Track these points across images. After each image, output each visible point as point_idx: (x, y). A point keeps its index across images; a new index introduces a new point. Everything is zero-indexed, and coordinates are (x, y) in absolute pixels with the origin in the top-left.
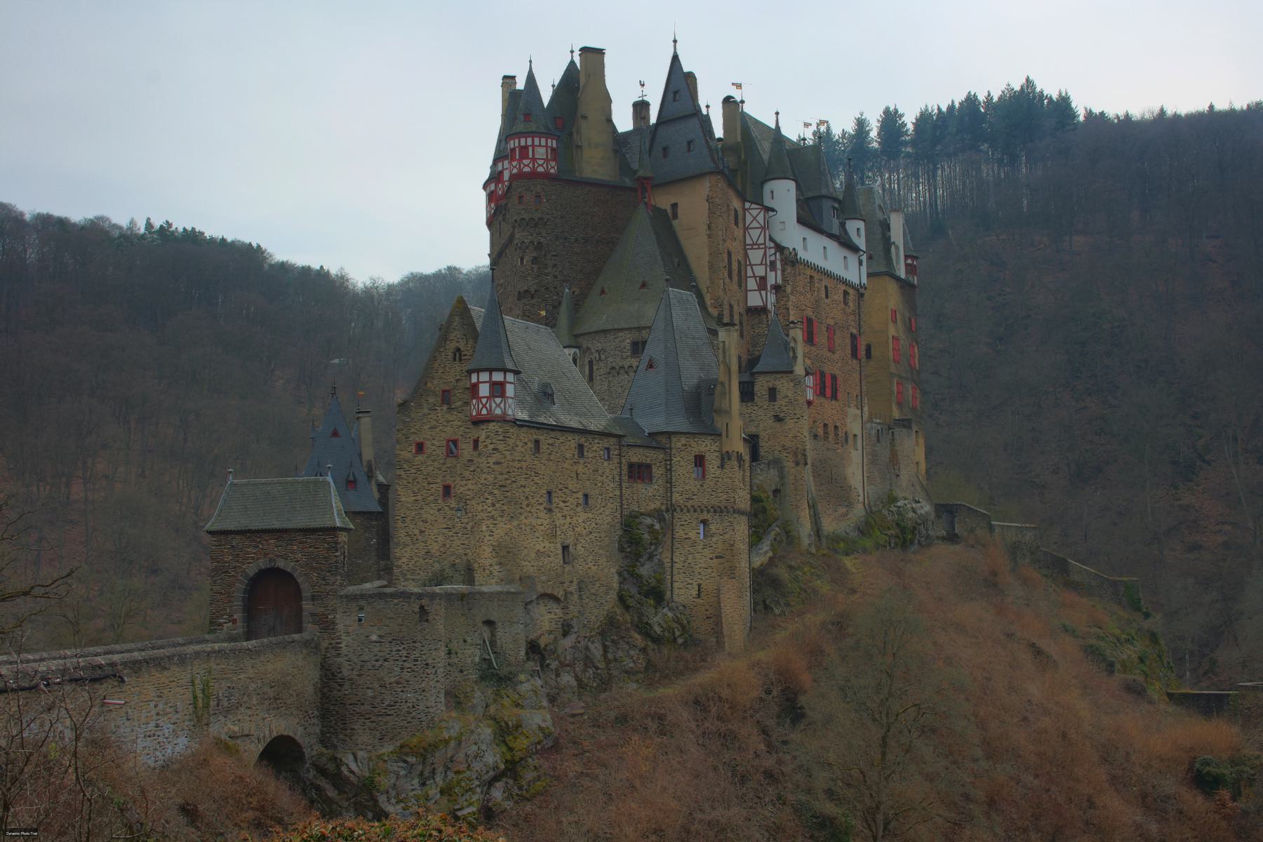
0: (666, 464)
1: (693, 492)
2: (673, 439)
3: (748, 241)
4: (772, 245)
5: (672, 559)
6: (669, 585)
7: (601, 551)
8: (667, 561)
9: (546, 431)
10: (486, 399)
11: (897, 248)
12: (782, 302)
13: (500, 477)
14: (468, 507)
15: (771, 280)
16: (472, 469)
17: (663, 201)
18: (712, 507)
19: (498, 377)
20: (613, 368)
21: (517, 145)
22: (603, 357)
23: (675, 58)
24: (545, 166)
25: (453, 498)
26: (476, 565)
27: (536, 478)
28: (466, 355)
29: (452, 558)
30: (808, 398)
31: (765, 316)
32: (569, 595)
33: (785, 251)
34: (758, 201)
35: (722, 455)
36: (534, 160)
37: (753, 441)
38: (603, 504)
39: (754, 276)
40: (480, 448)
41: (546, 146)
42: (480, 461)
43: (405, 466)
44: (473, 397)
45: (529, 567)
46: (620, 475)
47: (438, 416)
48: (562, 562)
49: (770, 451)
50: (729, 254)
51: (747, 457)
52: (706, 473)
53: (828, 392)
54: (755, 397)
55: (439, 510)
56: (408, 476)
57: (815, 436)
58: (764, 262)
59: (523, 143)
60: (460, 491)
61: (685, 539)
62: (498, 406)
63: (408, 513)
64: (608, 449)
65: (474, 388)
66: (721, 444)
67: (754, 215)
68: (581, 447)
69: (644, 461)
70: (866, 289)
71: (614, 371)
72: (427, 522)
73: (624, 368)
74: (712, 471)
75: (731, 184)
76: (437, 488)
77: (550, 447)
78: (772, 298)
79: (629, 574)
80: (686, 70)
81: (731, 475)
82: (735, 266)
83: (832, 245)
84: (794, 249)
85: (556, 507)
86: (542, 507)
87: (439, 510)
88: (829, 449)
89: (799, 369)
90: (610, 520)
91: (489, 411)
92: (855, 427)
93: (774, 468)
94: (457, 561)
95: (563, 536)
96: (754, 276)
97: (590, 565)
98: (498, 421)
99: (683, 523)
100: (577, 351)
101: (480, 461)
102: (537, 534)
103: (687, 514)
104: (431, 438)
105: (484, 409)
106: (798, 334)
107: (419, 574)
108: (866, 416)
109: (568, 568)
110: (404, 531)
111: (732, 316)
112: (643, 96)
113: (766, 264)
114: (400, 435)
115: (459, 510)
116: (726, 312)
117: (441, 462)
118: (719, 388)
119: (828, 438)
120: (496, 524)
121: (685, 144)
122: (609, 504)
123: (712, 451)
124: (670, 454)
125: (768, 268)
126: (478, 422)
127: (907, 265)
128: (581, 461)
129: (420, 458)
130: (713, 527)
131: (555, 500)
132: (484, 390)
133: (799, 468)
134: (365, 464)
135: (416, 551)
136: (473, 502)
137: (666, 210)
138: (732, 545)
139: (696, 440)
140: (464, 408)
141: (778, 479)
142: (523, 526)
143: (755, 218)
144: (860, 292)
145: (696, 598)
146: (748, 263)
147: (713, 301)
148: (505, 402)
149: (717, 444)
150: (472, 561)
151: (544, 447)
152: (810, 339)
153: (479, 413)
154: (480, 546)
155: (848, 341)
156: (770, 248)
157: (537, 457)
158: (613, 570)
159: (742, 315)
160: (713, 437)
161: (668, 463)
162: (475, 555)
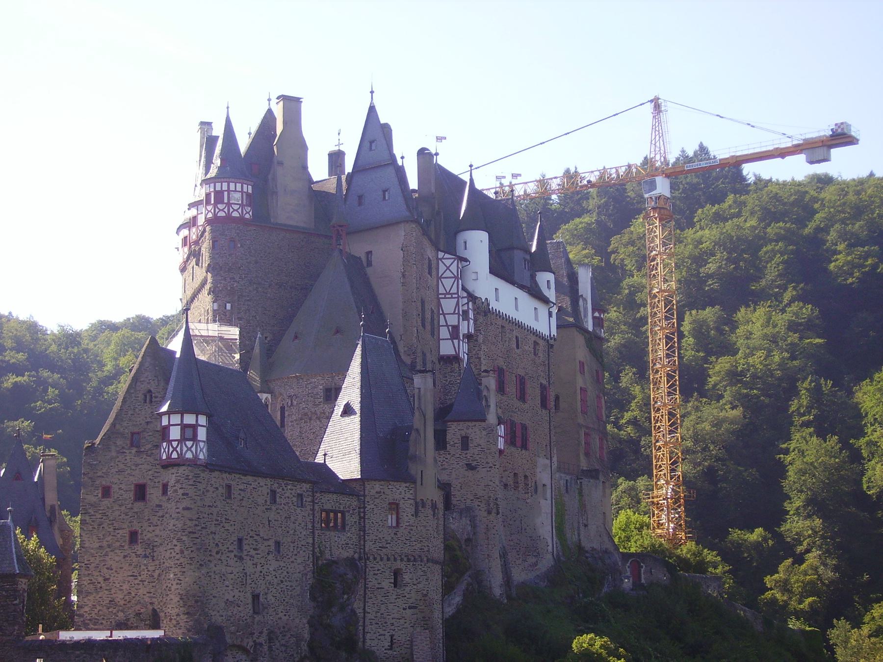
0: (359, 512)
1: (386, 540)
2: (366, 485)
3: (441, 290)
4: (465, 295)
5: (364, 609)
6: (361, 636)
7: (292, 601)
8: (359, 612)
9: (238, 476)
10: (177, 442)
11: (585, 300)
12: (474, 352)
13: (189, 523)
14: (155, 554)
15: (464, 329)
16: (160, 514)
17: (358, 248)
18: (405, 556)
20: (306, 414)
21: (212, 190)
22: (295, 403)
23: (372, 110)
24: (240, 211)
25: (140, 545)
26: (162, 615)
27: (227, 526)
28: (156, 397)
29: (138, 607)
30: (499, 447)
31: (457, 365)
32: (258, 647)
33: (477, 301)
34: (451, 249)
35: (416, 503)
36: (229, 204)
37: (445, 488)
38: (295, 552)
39: (447, 326)
40: (169, 493)
41: (242, 192)
42: (169, 506)
43: (90, 511)
44: (164, 440)
45: (218, 618)
46: (313, 523)
47: (126, 459)
48: (251, 612)
49: (462, 499)
50: (423, 302)
51: (441, 506)
52: (400, 521)
53: (519, 441)
54: (448, 445)
55: (125, 557)
56: (93, 521)
57: (506, 486)
58: (457, 312)
59: (218, 188)
60: (147, 537)
61: (378, 588)
62: (189, 449)
63: (92, 559)
64: (300, 496)
66: (415, 492)
67: (447, 264)
68: (273, 493)
69: (337, 509)
70: (555, 340)
72: (112, 569)
73: (316, 414)
74: (406, 519)
75: (425, 233)
76: (125, 533)
77: (242, 493)
78: (464, 347)
80: (382, 121)
81: (425, 524)
82: (428, 315)
83: (522, 296)
84: (486, 299)
85: (247, 555)
86: (232, 555)
87: (125, 557)
88: (518, 499)
89: (492, 418)
90: (302, 569)
91: (180, 455)
92: (544, 477)
93: (466, 517)
94: (142, 611)
95: (253, 585)
96: (447, 326)
97: (281, 615)
98: (189, 465)
99: (376, 572)
100: (269, 396)
101: (169, 506)
102: (227, 583)
103: (380, 563)
104: (118, 482)
105: (175, 452)
106: (490, 382)
107: (102, 623)
108: (555, 466)
109: (258, 618)
110: (88, 578)
111: (424, 364)
112: (339, 145)
113: (458, 314)
114: (86, 479)
115: (146, 556)
116: (419, 361)
117: (130, 506)
119: (518, 487)
120: (184, 572)
121: (381, 193)
122: (301, 552)
123: (406, 499)
124: (364, 501)
125: (461, 317)
127: (594, 318)
128: (273, 507)
129: (106, 502)
130: (407, 577)
131: (245, 547)
132: (175, 433)
133: (492, 517)
134: (48, 508)
135: (100, 600)
136: (161, 549)
137: (360, 258)
138: (426, 595)
139: (390, 487)
140: (154, 451)
141: (469, 528)
142: (212, 574)
143: (448, 268)
144: (550, 343)
145: (388, 649)
146: (441, 312)
147: (406, 349)
148: (196, 446)
149: (411, 492)
150: (158, 610)
151: (235, 492)
152: (501, 389)
153: (169, 456)
154: (168, 595)
155: (538, 392)
156: (463, 297)
157: (227, 503)
158: (305, 621)
159: (434, 363)
160: (407, 485)
161: (362, 510)
162: (162, 604)
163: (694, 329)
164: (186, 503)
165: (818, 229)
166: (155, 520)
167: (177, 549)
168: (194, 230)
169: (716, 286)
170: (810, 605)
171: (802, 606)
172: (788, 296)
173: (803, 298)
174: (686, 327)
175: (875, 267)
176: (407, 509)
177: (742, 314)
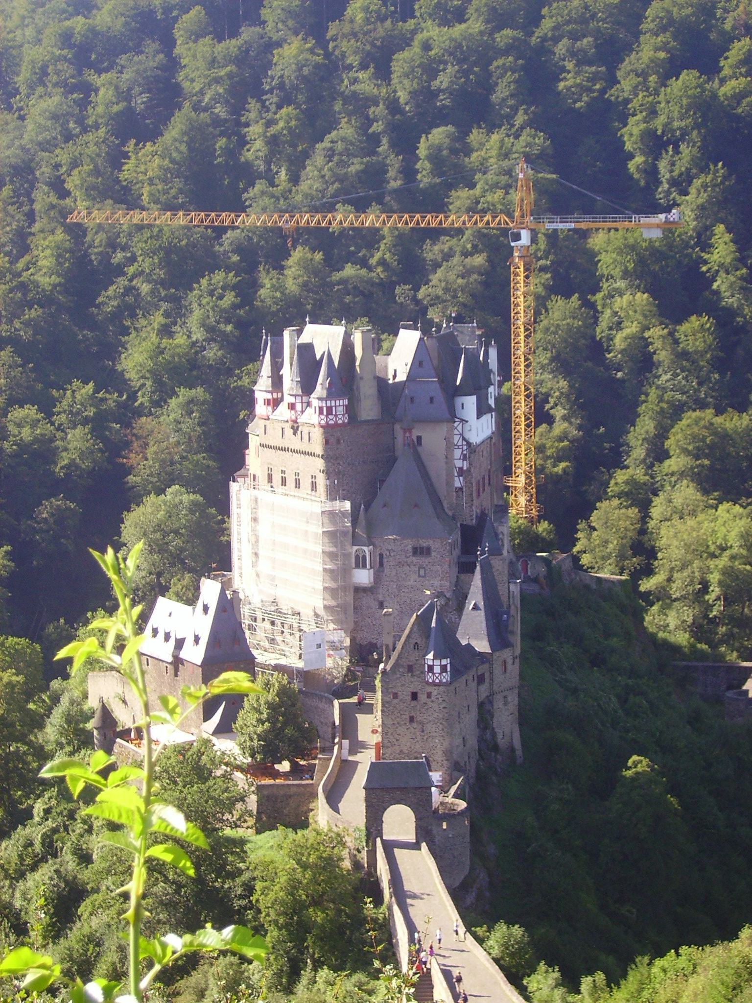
11: (494, 374)
19: (444, 662)
21: (324, 405)
36: (336, 415)
44: (429, 672)
59: (329, 405)
65: (431, 668)
71: (400, 564)
76: (407, 717)
79: (481, 740)
91: (440, 681)
118: (511, 619)
126: (427, 683)
129: (396, 701)
130: (509, 699)
132: (437, 669)
153: (434, 681)
163: (430, 154)
164: (444, 705)
165: (544, 39)
166: (423, 710)
167: (441, 727)
168: (293, 412)
169: (447, 102)
170: (564, 470)
171: (556, 469)
172: (520, 119)
173: (534, 123)
174: (422, 150)
175: (603, 91)
176: (510, 661)
177: (475, 136)
